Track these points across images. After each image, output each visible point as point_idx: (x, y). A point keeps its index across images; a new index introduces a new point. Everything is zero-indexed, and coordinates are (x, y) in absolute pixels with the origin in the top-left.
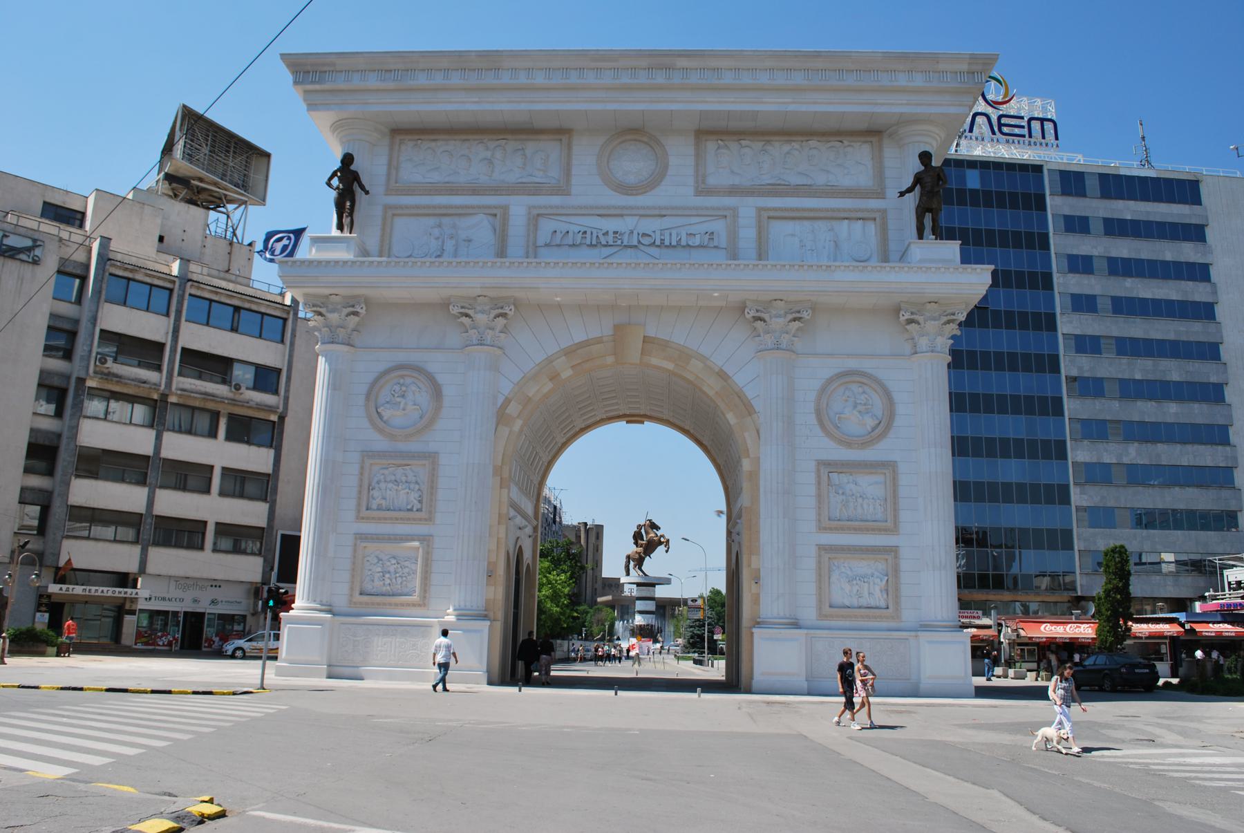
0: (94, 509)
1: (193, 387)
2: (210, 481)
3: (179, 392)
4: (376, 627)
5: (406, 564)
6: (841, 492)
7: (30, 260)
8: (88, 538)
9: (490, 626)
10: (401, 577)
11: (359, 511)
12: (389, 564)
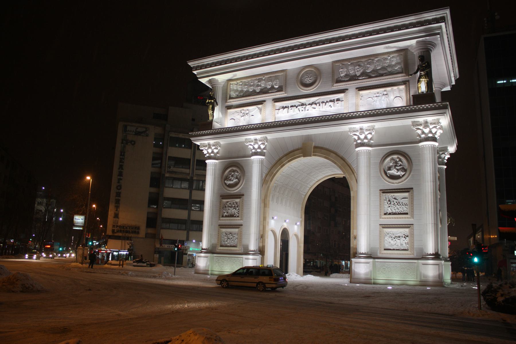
0: (170, 219)
1: (202, 173)
3: (196, 176)
4: (225, 258)
5: (234, 235)
6: (389, 203)
7: (145, 135)
8: (169, 229)
9: (262, 258)
10: (233, 240)
11: (220, 217)
12: (229, 236)
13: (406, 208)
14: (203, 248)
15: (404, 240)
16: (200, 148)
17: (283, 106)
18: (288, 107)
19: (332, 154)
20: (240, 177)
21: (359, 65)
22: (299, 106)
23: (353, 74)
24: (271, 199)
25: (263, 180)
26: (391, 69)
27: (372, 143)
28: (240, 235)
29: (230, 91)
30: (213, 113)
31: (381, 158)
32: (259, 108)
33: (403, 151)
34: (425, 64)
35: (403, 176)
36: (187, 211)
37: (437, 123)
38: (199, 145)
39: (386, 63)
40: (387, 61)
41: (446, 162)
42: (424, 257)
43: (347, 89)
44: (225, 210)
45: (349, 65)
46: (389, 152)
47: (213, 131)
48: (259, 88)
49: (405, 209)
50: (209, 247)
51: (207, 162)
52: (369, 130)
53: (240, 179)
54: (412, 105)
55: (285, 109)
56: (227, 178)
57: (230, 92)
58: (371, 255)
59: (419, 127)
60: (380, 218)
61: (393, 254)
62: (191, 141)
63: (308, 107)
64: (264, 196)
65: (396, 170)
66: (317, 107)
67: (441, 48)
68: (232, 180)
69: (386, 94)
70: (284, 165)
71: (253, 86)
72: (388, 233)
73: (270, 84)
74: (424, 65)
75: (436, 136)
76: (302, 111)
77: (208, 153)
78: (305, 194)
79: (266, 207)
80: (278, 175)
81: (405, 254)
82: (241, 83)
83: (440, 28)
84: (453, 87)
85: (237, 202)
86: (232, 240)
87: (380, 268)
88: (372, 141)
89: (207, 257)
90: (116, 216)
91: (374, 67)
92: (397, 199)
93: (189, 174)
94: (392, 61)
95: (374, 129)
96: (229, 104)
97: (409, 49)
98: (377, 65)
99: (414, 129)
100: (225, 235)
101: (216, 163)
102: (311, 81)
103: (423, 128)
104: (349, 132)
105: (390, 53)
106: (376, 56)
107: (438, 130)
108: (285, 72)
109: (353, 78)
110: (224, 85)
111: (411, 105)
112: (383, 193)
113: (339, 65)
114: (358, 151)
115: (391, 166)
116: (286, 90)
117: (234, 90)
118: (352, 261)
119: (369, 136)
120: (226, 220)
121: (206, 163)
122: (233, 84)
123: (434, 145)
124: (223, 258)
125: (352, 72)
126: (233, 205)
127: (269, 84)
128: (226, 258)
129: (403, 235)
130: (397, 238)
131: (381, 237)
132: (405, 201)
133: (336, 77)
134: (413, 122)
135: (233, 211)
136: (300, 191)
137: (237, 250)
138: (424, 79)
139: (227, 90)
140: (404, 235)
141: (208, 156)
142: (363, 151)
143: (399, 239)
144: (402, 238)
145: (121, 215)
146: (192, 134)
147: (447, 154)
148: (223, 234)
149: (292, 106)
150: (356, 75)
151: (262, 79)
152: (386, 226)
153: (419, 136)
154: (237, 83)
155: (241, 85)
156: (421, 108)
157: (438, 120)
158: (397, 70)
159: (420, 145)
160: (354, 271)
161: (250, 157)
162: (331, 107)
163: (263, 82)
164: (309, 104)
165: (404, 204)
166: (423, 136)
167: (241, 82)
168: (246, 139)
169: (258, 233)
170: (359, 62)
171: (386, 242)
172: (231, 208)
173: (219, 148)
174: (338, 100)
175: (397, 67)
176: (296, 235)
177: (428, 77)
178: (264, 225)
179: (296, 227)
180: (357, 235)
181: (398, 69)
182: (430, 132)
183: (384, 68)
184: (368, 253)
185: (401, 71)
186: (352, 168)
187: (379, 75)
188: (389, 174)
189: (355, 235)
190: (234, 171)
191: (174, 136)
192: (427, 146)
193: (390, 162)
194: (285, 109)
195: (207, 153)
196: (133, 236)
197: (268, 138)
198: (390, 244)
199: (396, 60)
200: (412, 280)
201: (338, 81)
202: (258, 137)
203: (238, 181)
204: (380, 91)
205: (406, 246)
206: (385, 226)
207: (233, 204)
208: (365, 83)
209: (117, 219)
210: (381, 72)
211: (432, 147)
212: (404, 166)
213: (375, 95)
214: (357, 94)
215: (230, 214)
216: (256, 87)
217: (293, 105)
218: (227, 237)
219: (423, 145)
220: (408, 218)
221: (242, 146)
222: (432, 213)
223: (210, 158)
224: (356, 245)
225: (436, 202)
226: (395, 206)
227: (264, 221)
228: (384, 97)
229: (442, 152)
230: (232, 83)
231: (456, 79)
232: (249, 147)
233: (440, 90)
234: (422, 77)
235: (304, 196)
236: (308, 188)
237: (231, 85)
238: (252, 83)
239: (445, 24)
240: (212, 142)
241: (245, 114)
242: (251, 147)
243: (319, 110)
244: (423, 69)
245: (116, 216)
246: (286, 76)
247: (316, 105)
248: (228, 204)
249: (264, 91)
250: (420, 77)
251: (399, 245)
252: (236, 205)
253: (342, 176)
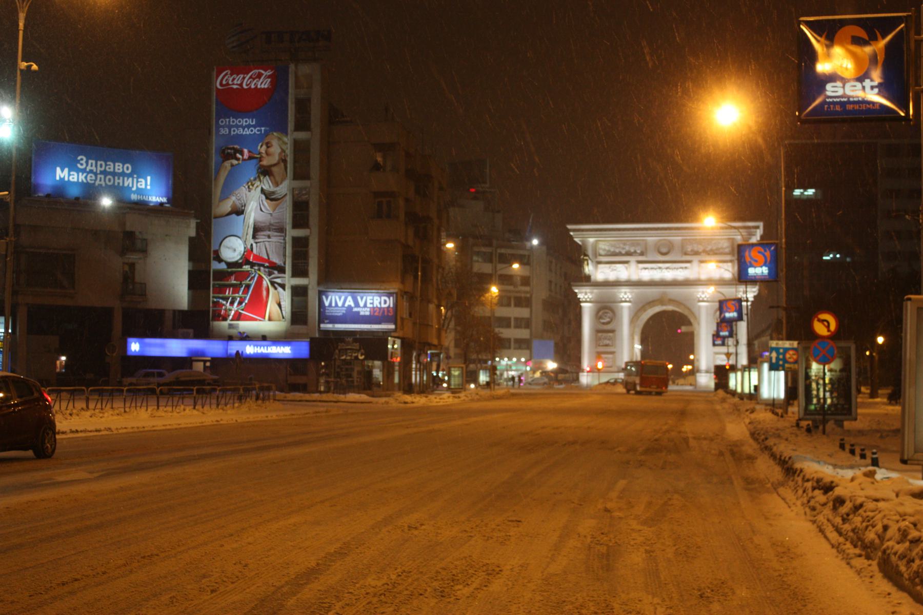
2: (510, 323)
56: (601, 318)
63: (664, 270)
66: (670, 271)
71: (617, 248)
109: (696, 253)
117: (602, 249)
125: (696, 249)
131: (714, 359)
135: (607, 342)
174: (686, 268)
194: (647, 270)
201: (686, 254)
202: (627, 290)
210: (716, 252)
223: (586, 302)
230: (600, 243)
242: (621, 297)
249: (629, 254)
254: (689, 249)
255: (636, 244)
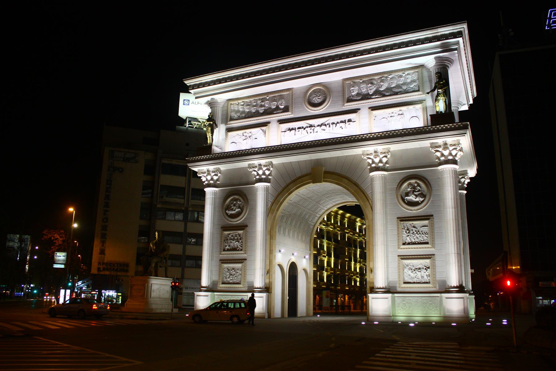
4: (227, 296)
6: (407, 232)
7: (135, 162)
12: (231, 272)
13: (426, 237)
14: (203, 286)
15: (425, 272)
16: (198, 175)
17: (290, 128)
18: (295, 129)
19: (344, 179)
20: (243, 206)
21: (372, 83)
22: (307, 127)
23: (365, 92)
24: (277, 231)
25: (268, 209)
26: (406, 86)
27: (388, 167)
28: (244, 271)
29: (231, 112)
30: (212, 136)
31: (397, 184)
32: (263, 130)
33: (422, 175)
34: (443, 81)
35: (422, 202)
36: (182, 246)
37: (457, 145)
38: (197, 171)
39: (401, 81)
40: (402, 79)
41: (466, 186)
42: (447, 291)
43: (359, 109)
44: (226, 243)
45: (361, 83)
46: (406, 176)
47: (213, 156)
48: (264, 108)
49: (425, 238)
50: (209, 284)
51: (205, 191)
52: (385, 153)
53: (243, 209)
54: (430, 125)
55: (292, 131)
56: (228, 208)
57: (231, 113)
58: (389, 290)
59: (438, 149)
60: (399, 248)
61: (413, 287)
62: (187, 166)
64: (270, 227)
65: (414, 196)
67: (458, 64)
68: (234, 209)
69: (402, 114)
70: (291, 192)
72: (407, 264)
73: (275, 104)
74: (441, 83)
75: (457, 159)
76: (311, 133)
77: (207, 180)
78: (314, 224)
79: (273, 239)
80: (285, 203)
81: (427, 287)
82: (242, 103)
83: (458, 43)
84: (471, 106)
85: (240, 234)
86: (235, 276)
87: (399, 303)
88: (387, 165)
89: (207, 296)
90: (102, 252)
91: (388, 85)
92: (416, 227)
93: (184, 204)
94: (408, 78)
95: (389, 151)
96: (230, 126)
97: (425, 65)
98: (392, 83)
99: (433, 151)
100: (227, 270)
101: (216, 191)
102: (320, 101)
103: (442, 150)
104: (362, 155)
105: (404, 70)
106: (389, 73)
107: (458, 152)
108: (291, 92)
109: (366, 97)
110: (223, 105)
111: (429, 125)
112: (401, 221)
113: (351, 83)
114: (372, 176)
115: (409, 191)
116: (292, 111)
117: (234, 111)
118: (369, 296)
119: (385, 160)
120: (228, 254)
121: (205, 192)
122: (234, 105)
123: (454, 168)
124: (225, 296)
125: (364, 91)
126: (236, 238)
127: (273, 104)
128: (229, 296)
129: (423, 266)
130: (417, 271)
132: (425, 229)
133: (347, 96)
134: (432, 144)
135: (236, 244)
136: (309, 222)
137: (241, 287)
138: (442, 98)
139: (227, 111)
140: (425, 266)
141: (207, 184)
142: (378, 176)
143: (420, 271)
144: (423, 270)
145: (107, 251)
146: (189, 160)
147: (467, 178)
148: (225, 270)
149: (299, 128)
150: (368, 94)
151: (266, 99)
152: (405, 257)
153: (438, 158)
154: (238, 103)
155: (243, 105)
156: (440, 128)
157: (458, 140)
158: (412, 88)
159: (440, 169)
160: (372, 307)
161: (254, 184)
162: (342, 128)
163: (267, 102)
164: (318, 126)
165: (424, 232)
166: (442, 158)
167: (243, 102)
168: (249, 165)
169: (264, 268)
170: (372, 79)
171: (405, 274)
172: (234, 241)
173: (219, 175)
174: (350, 121)
175: (412, 84)
176: (305, 270)
177: (446, 95)
178: (271, 259)
179: (304, 260)
180: (373, 268)
181: (414, 87)
182: (450, 154)
183: (398, 86)
184: (386, 287)
185: (417, 89)
186: (366, 195)
187: (393, 94)
188: (407, 201)
189: (371, 268)
190: (236, 200)
191: (167, 162)
192: (447, 169)
193: (407, 187)
194: (293, 131)
195: (205, 180)
196: (121, 275)
197: (274, 163)
198: (410, 276)
199: (411, 78)
200: (435, 316)
201: (349, 100)
202: (263, 162)
203: (241, 211)
204: (395, 110)
205: (427, 278)
206: (403, 257)
207: (236, 236)
208: (378, 102)
209: (103, 256)
210: (397, 90)
211: (453, 170)
212: (422, 192)
213: (390, 115)
214: (370, 114)
215: (232, 248)
216: (259, 107)
217: (301, 126)
218: (230, 273)
219: (443, 169)
220: (428, 248)
221: (244, 173)
222: (454, 242)
223: (209, 185)
224: (373, 279)
225: (459, 230)
226: (414, 235)
227: (271, 255)
228: (400, 117)
229: (462, 176)
230: (232, 103)
231: (474, 98)
232: (252, 173)
233: (457, 110)
234: (440, 96)
235: (313, 227)
236: (317, 218)
237: (232, 106)
238: (255, 103)
239: (463, 39)
240: (211, 168)
241: (248, 137)
242: (255, 173)
243: (329, 132)
244: (441, 86)
245: (102, 252)
246: (292, 95)
247: (326, 126)
248: (230, 236)
249: (269, 112)
250: (438, 95)
251: (420, 278)
252: (239, 238)
253: (354, 204)
254: (355, 91)
255: (277, 95)
